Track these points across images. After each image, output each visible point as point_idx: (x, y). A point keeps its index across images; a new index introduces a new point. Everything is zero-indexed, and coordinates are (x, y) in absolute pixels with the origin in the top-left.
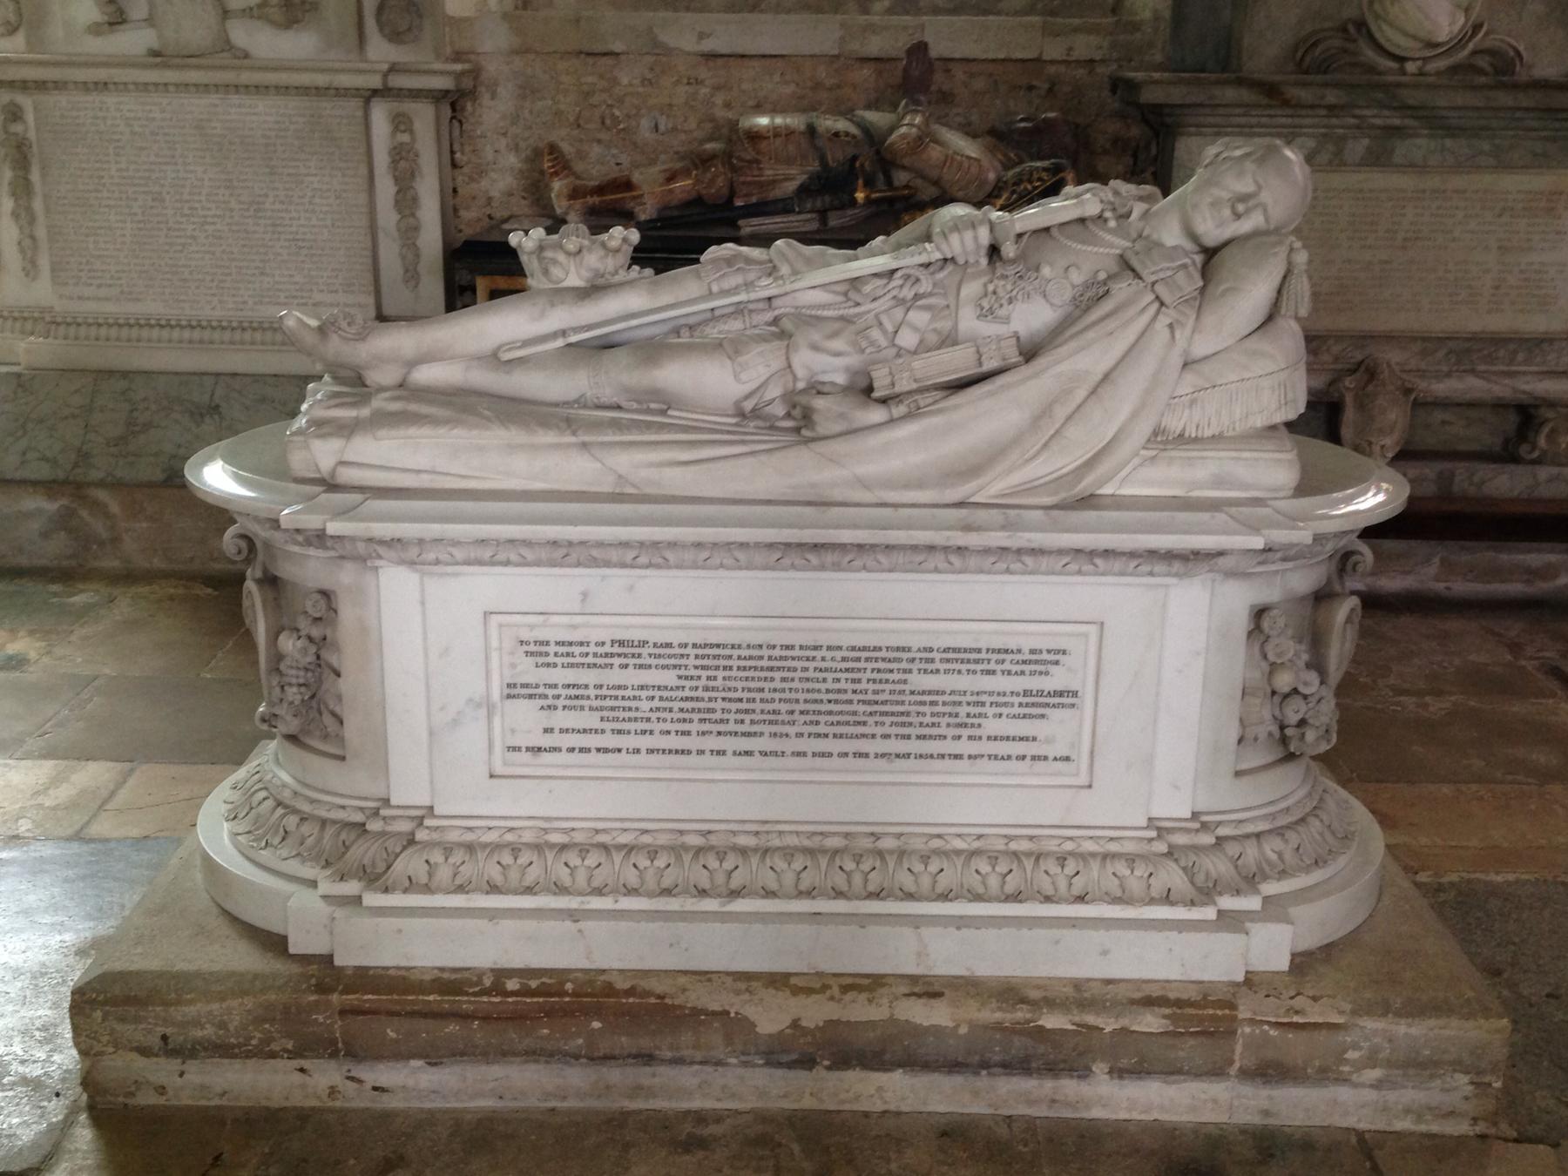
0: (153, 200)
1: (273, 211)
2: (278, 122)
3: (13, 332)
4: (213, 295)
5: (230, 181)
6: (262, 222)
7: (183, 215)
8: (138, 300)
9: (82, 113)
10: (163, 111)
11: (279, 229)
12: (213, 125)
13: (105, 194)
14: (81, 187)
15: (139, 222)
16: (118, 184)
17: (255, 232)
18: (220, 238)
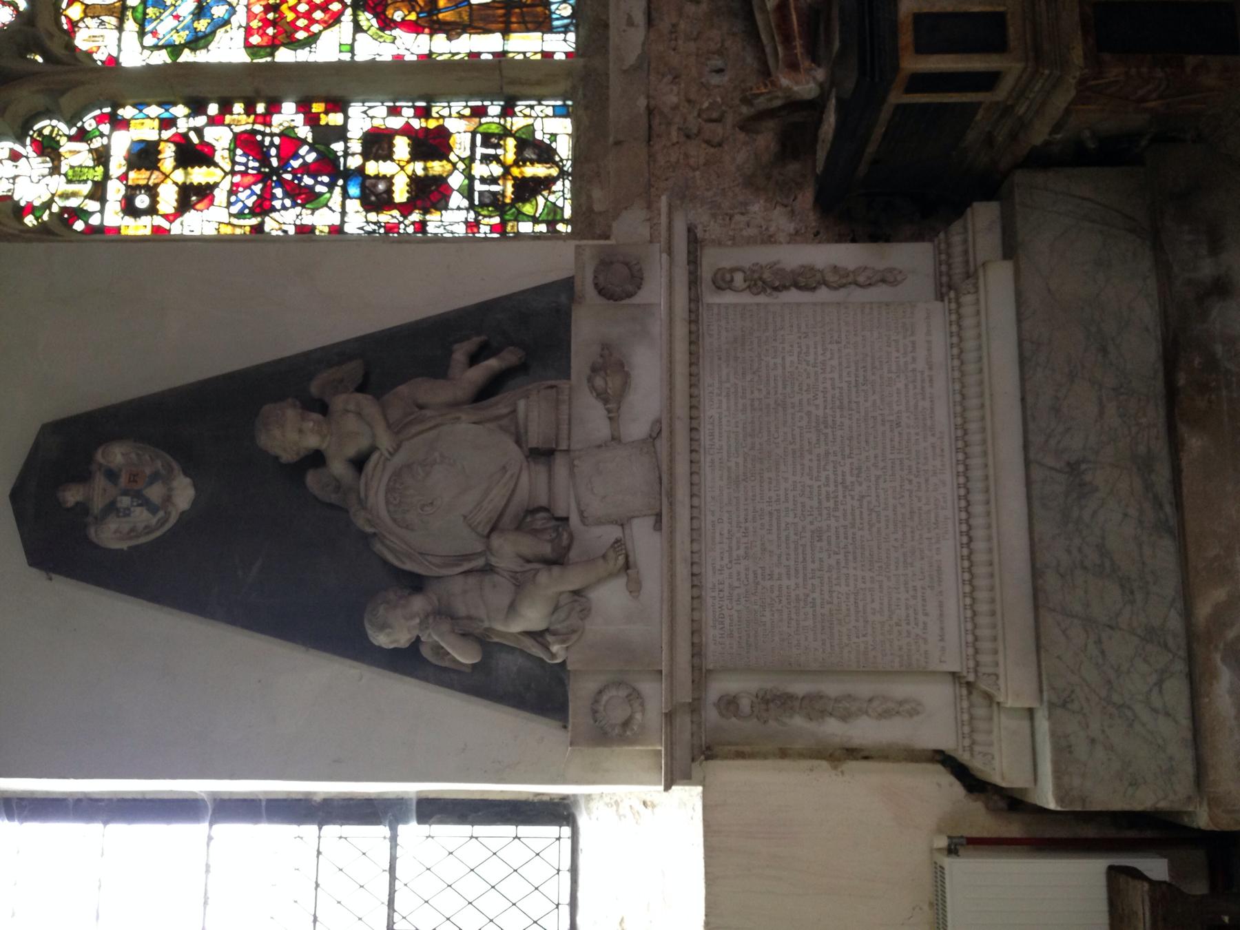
0: (820, 540)
1: (825, 408)
2: (728, 395)
3: (991, 744)
4: (927, 480)
5: (794, 452)
6: (838, 421)
7: (836, 509)
8: (939, 569)
9: (726, 612)
10: (720, 520)
11: (846, 401)
12: (732, 464)
13: (816, 595)
14: (810, 623)
15: (847, 560)
16: (805, 580)
17: (850, 427)
18: (859, 469)
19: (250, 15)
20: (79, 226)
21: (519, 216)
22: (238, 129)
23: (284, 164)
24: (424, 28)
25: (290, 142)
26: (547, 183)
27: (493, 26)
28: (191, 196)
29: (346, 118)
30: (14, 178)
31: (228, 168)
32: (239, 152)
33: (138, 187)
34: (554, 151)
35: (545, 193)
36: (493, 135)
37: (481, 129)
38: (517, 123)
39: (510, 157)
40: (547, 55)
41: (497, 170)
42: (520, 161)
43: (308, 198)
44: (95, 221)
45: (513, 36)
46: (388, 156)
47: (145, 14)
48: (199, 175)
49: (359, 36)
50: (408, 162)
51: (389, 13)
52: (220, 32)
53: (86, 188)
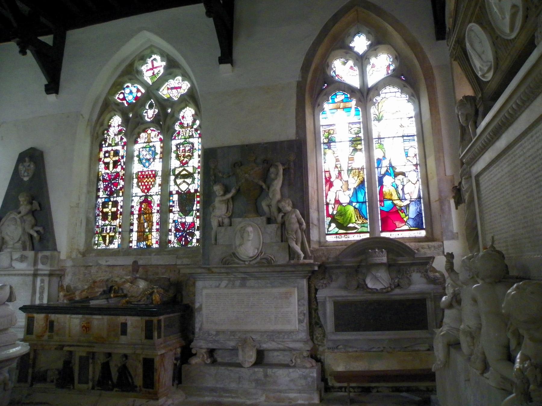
19: (145, 172)
20: (103, 143)
21: (99, 237)
22: (120, 173)
23: (113, 184)
24: (140, 212)
25: (116, 184)
26: (105, 243)
27: (139, 229)
28: (107, 165)
29: (121, 196)
30: (114, 127)
31: (112, 172)
32: (115, 174)
33: (110, 153)
34: (111, 244)
35: (103, 243)
36: (115, 230)
37: (117, 227)
38: (117, 236)
39: (111, 234)
40: (131, 242)
41: (108, 231)
42: (110, 237)
43: (105, 189)
44: (104, 146)
45: (137, 233)
46: (112, 207)
47: (147, 148)
48: (111, 166)
49: (139, 197)
50: (111, 211)
51: (144, 204)
52: (142, 165)
53: (110, 142)
